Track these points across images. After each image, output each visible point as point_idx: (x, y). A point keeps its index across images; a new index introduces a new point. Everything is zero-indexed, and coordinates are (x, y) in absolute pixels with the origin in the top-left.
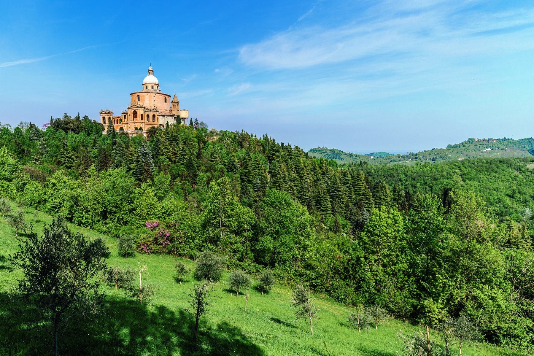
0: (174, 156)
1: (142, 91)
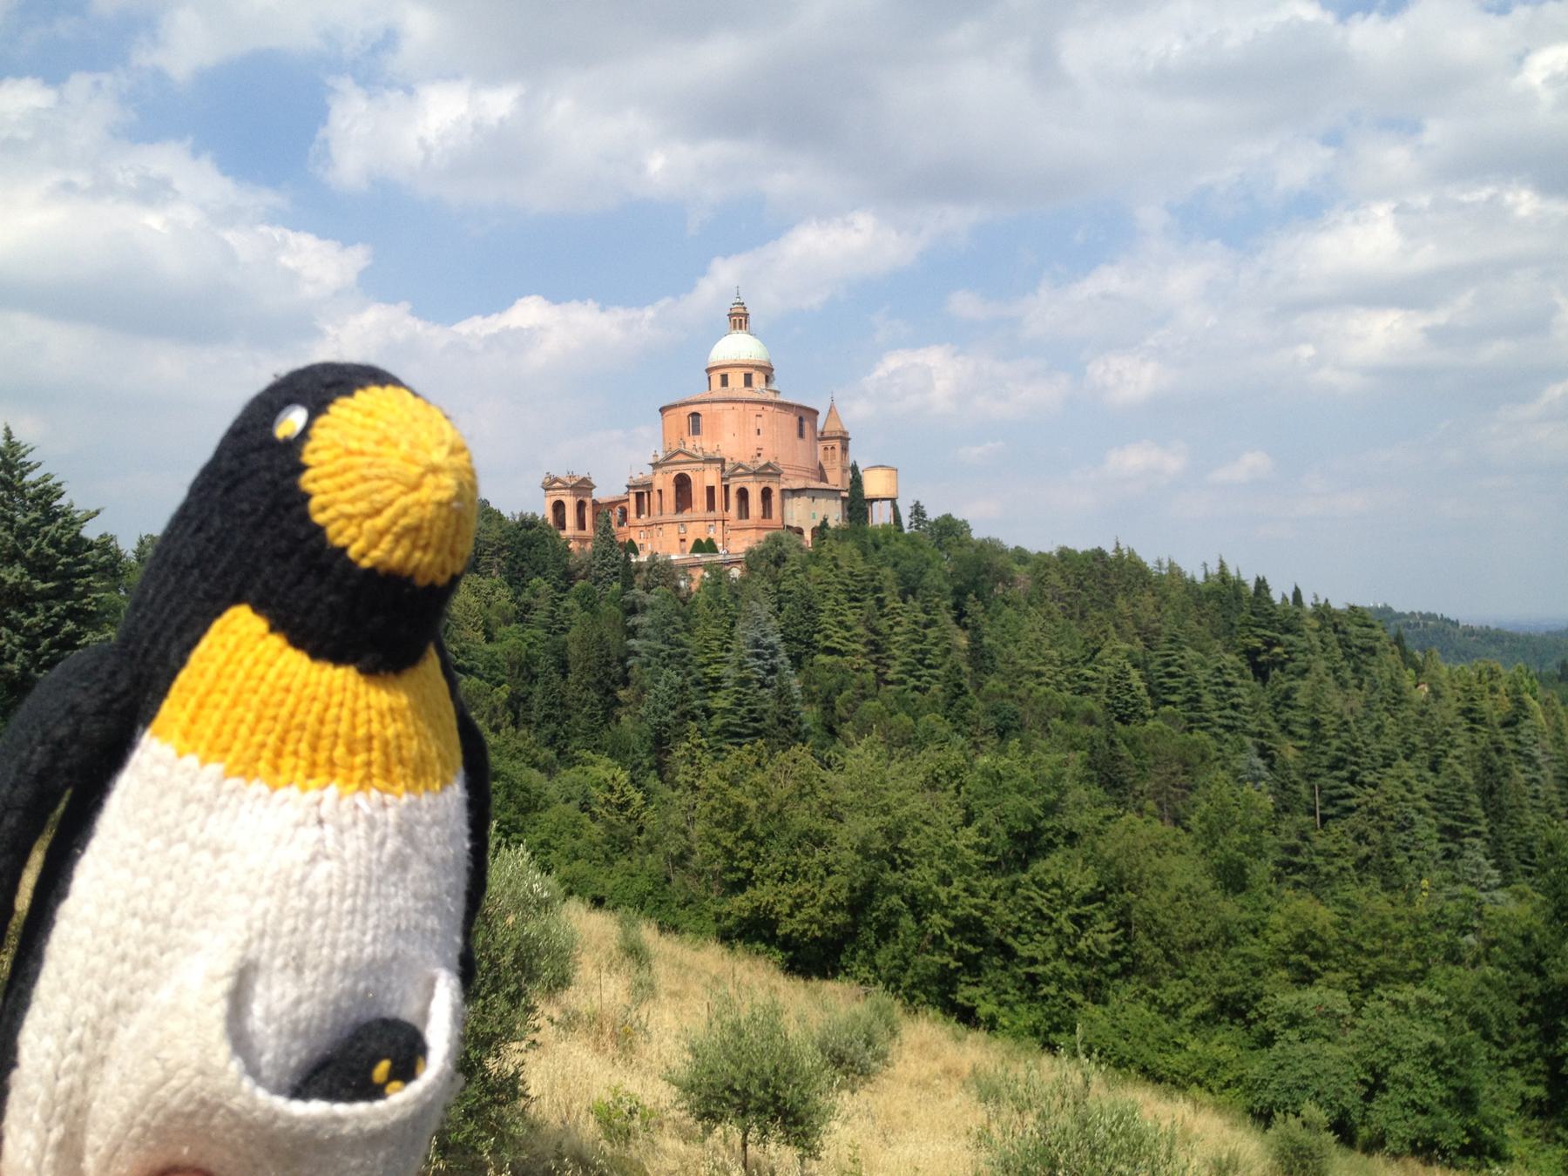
0: (874, 657)
1: (709, 397)
